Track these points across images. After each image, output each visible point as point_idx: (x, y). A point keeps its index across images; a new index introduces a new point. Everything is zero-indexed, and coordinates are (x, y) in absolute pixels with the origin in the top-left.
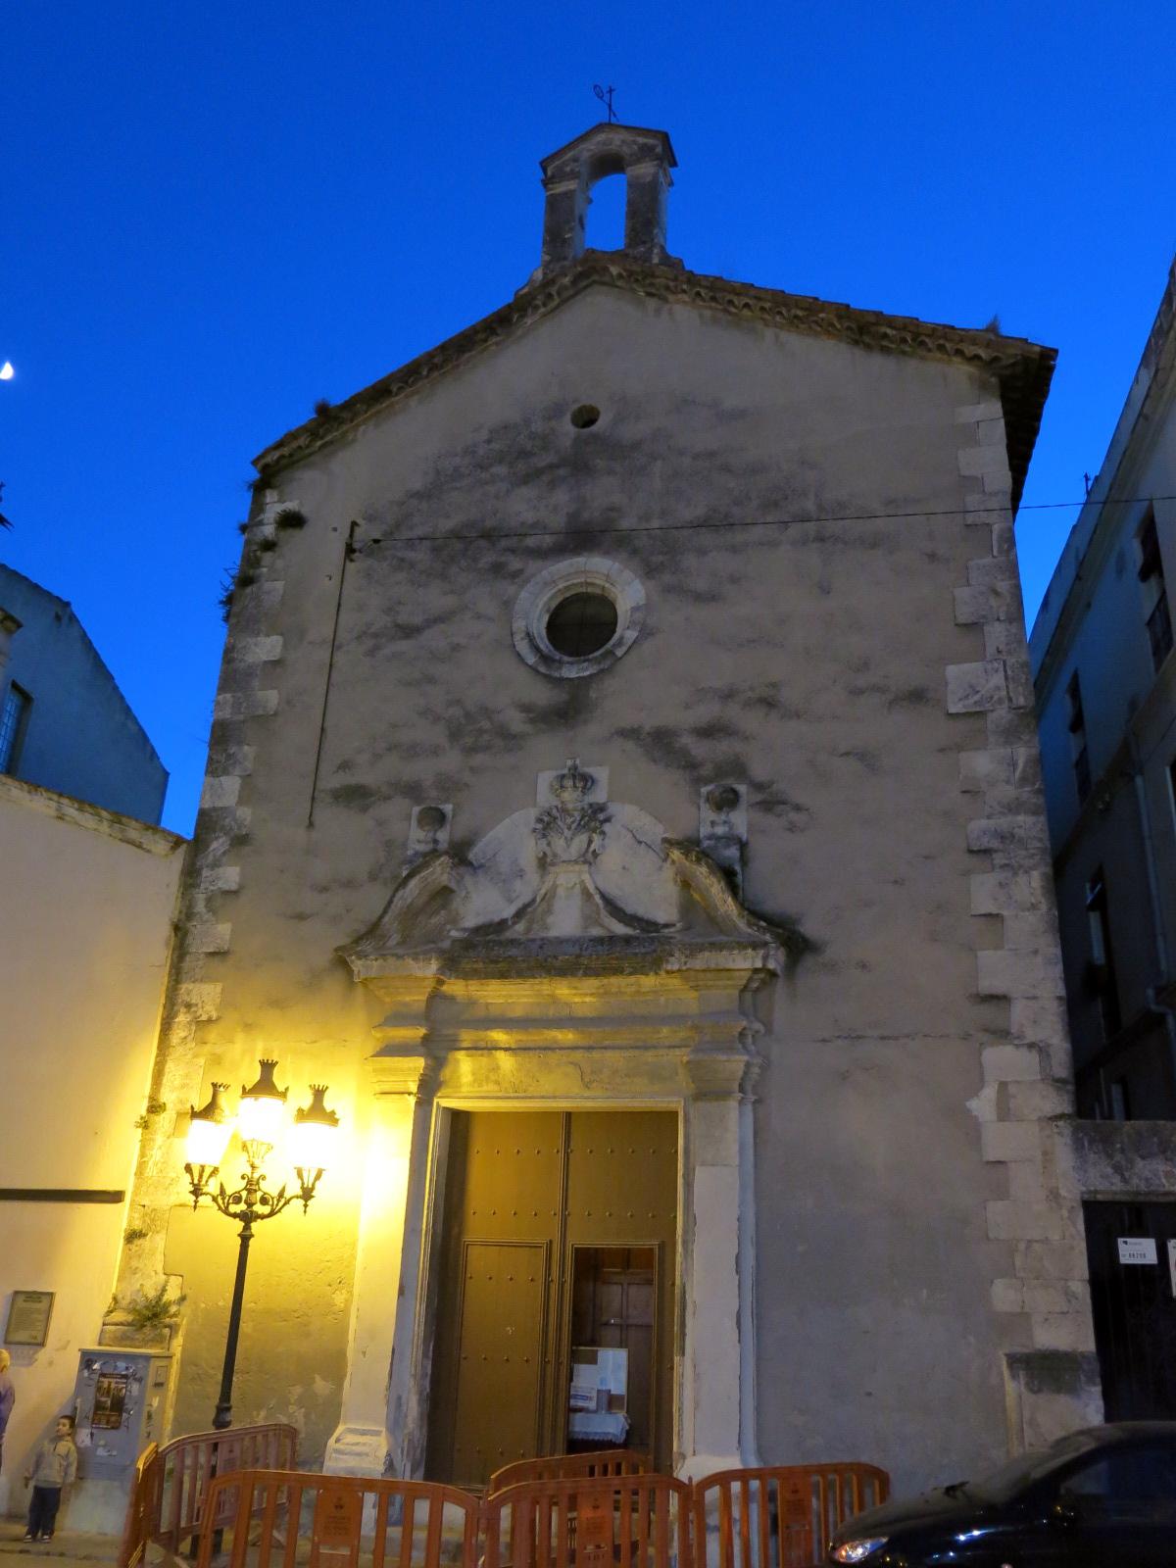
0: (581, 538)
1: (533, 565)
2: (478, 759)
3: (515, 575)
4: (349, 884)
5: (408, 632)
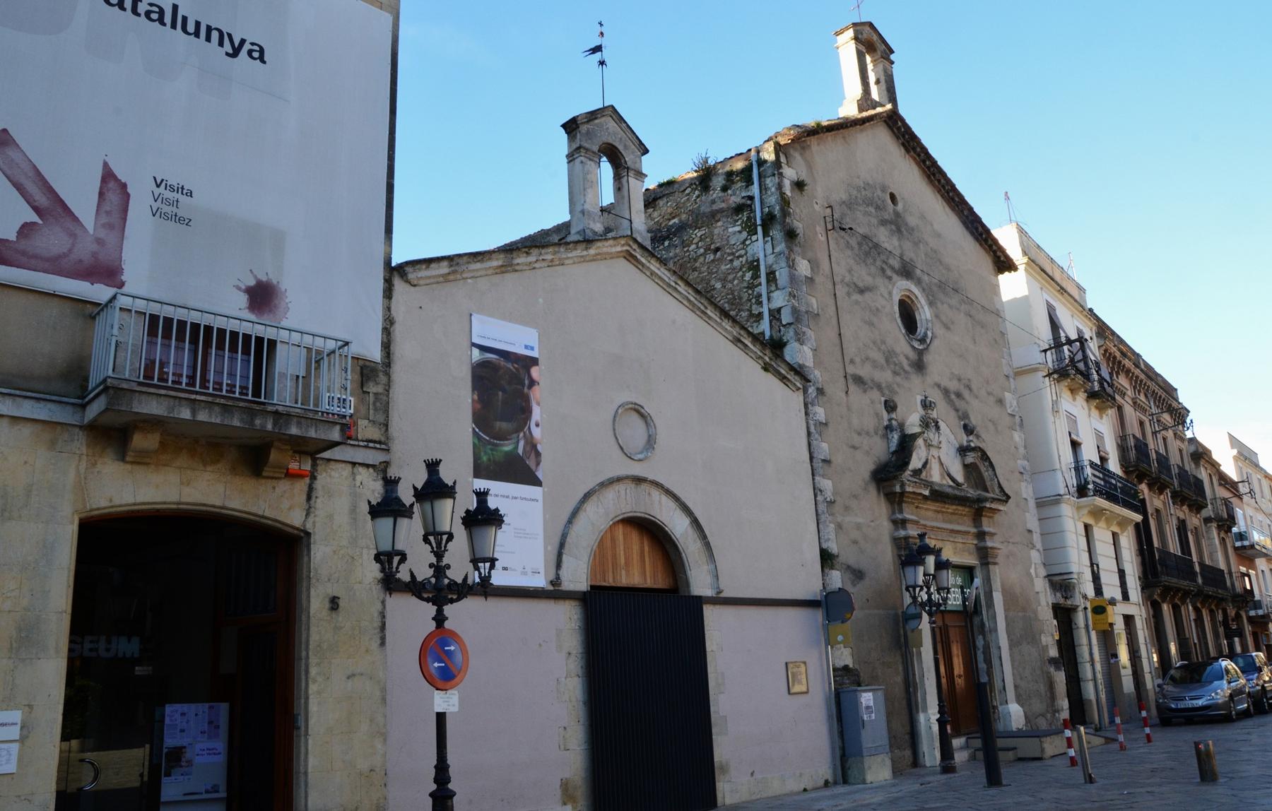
0: (906, 271)
1: (895, 277)
2: (898, 379)
3: (890, 278)
4: (868, 433)
5: (862, 291)
